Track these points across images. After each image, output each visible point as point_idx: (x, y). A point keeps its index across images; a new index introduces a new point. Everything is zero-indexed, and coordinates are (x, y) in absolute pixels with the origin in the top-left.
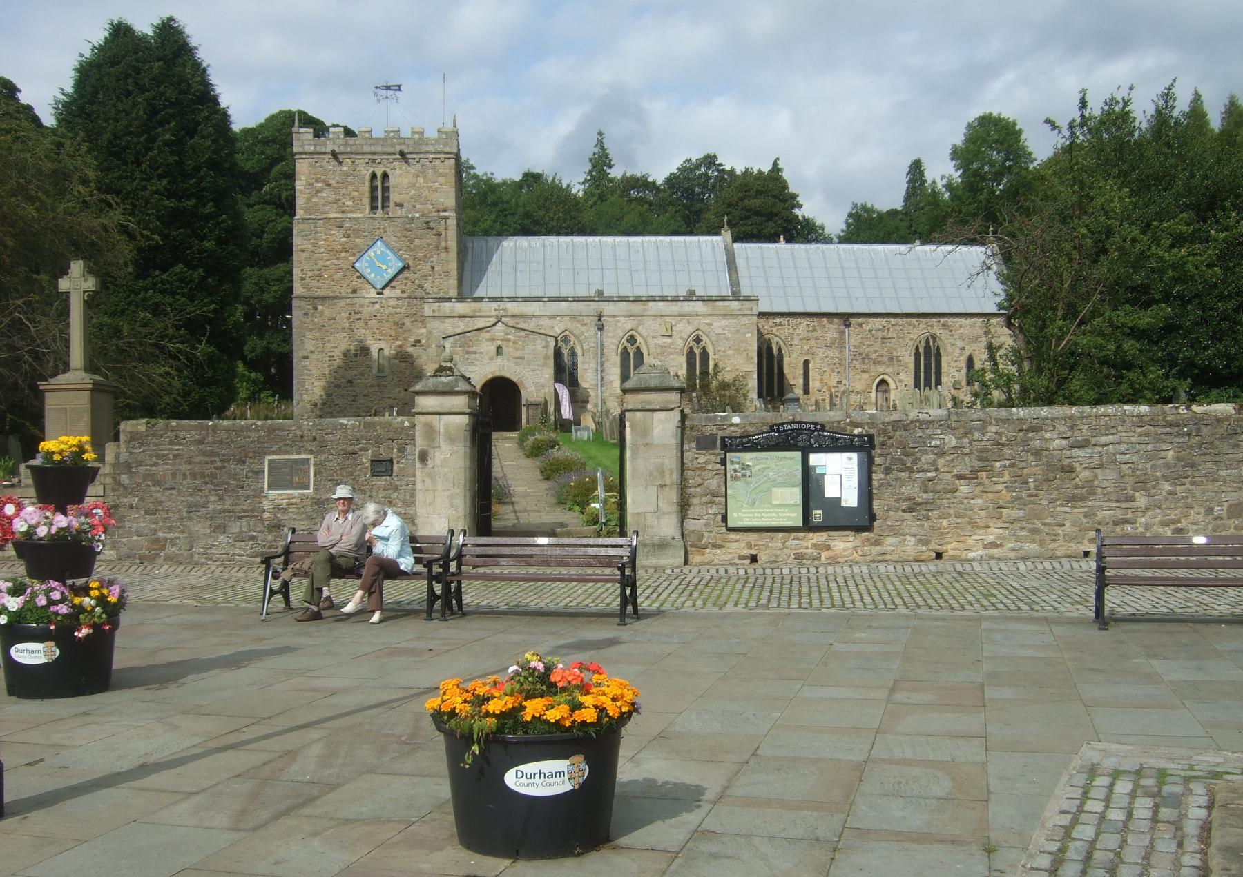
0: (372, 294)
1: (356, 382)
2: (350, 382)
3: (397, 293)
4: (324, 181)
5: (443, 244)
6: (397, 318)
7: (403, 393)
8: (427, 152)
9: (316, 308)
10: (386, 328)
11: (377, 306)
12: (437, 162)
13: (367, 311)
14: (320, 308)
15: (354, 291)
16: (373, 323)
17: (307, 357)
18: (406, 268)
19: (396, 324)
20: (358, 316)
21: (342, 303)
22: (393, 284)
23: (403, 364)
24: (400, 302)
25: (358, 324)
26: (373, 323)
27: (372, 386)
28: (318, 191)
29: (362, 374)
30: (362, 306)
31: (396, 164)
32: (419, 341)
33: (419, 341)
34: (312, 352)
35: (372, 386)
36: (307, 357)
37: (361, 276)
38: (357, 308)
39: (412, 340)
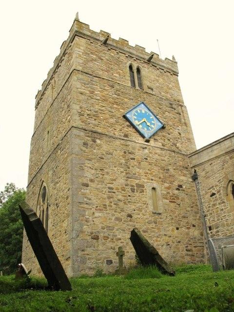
0: (141, 140)
1: (135, 216)
2: (130, 216)
3: (159, 145)
4: (96, 55)
5: (183, 121)
6: (163, 164)
7: (176, 231)
8: (163, 66)
9: (95, 142)
10: (156, 169)
11: (146, 151)
12: (169, 74)
13: (139, 154)
14: (98, 141)
15: (126, 136)
16: (144, 164)
17: (87, 185)
18: (163, 128)
19: (163, 169)
20: (132, 156)
21: (118, 142)
22: (156, 137)
23: (172, 205)
24: (164, 152)
25: (132, 163)
26: (144, 164)
27: (149, 223)
28: (92, 60)
29: (140, 210)
30: (134, 148)
31: (146, 65)
32: (180, 186)
33: (180, 186)
34: (92, 181)
35: (149, 223)
36: (87, 185)
37: (132, 125)
38: (131, 150)
39: (176, 184)
